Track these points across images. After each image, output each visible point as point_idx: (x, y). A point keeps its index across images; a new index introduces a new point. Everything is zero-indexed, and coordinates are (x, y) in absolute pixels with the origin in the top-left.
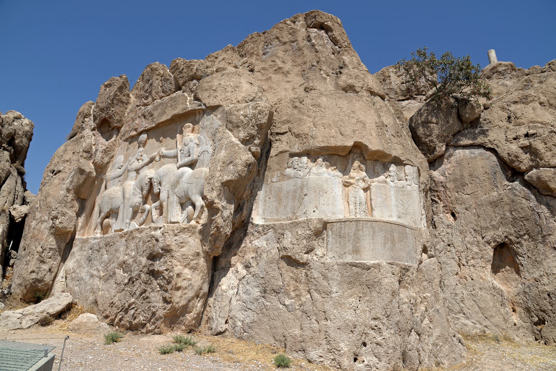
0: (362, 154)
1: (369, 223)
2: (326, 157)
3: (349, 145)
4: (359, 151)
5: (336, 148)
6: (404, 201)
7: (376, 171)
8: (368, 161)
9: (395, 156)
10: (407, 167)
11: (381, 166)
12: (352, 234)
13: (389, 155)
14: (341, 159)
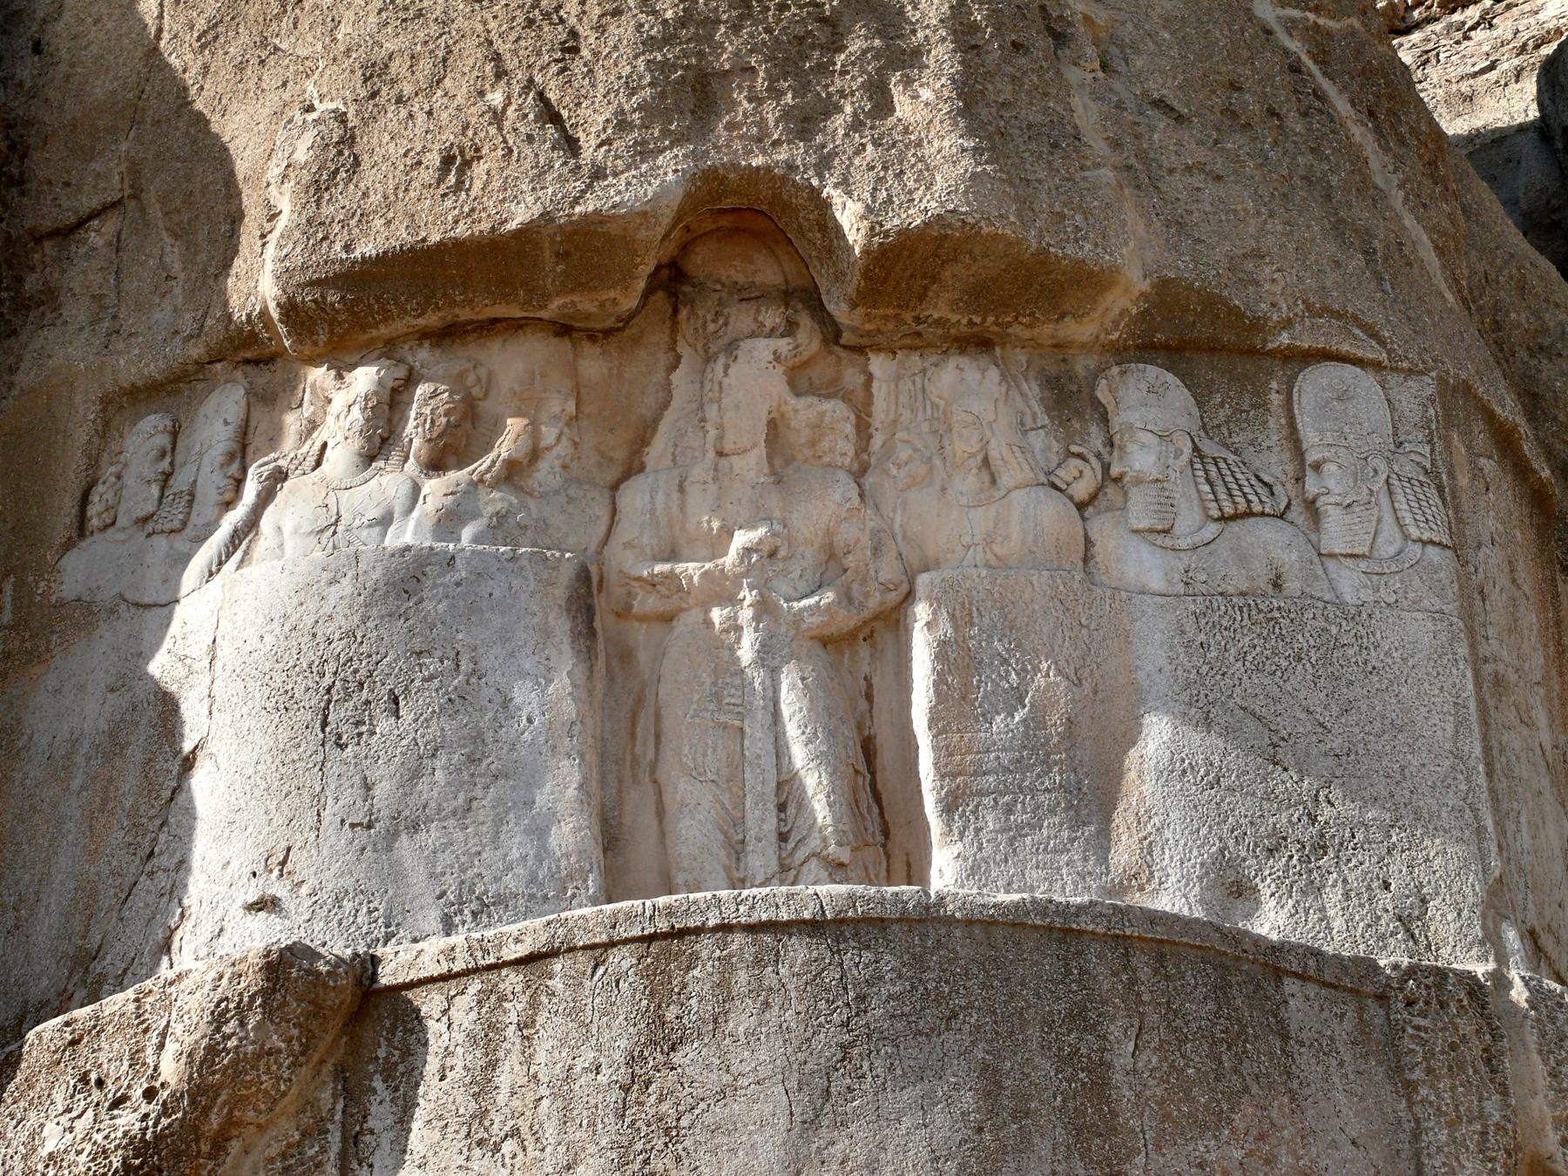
1: (799, 951)
8: (878, 364)
10: (1315, 384)
12: (597, 1090)
14: (593, 364)
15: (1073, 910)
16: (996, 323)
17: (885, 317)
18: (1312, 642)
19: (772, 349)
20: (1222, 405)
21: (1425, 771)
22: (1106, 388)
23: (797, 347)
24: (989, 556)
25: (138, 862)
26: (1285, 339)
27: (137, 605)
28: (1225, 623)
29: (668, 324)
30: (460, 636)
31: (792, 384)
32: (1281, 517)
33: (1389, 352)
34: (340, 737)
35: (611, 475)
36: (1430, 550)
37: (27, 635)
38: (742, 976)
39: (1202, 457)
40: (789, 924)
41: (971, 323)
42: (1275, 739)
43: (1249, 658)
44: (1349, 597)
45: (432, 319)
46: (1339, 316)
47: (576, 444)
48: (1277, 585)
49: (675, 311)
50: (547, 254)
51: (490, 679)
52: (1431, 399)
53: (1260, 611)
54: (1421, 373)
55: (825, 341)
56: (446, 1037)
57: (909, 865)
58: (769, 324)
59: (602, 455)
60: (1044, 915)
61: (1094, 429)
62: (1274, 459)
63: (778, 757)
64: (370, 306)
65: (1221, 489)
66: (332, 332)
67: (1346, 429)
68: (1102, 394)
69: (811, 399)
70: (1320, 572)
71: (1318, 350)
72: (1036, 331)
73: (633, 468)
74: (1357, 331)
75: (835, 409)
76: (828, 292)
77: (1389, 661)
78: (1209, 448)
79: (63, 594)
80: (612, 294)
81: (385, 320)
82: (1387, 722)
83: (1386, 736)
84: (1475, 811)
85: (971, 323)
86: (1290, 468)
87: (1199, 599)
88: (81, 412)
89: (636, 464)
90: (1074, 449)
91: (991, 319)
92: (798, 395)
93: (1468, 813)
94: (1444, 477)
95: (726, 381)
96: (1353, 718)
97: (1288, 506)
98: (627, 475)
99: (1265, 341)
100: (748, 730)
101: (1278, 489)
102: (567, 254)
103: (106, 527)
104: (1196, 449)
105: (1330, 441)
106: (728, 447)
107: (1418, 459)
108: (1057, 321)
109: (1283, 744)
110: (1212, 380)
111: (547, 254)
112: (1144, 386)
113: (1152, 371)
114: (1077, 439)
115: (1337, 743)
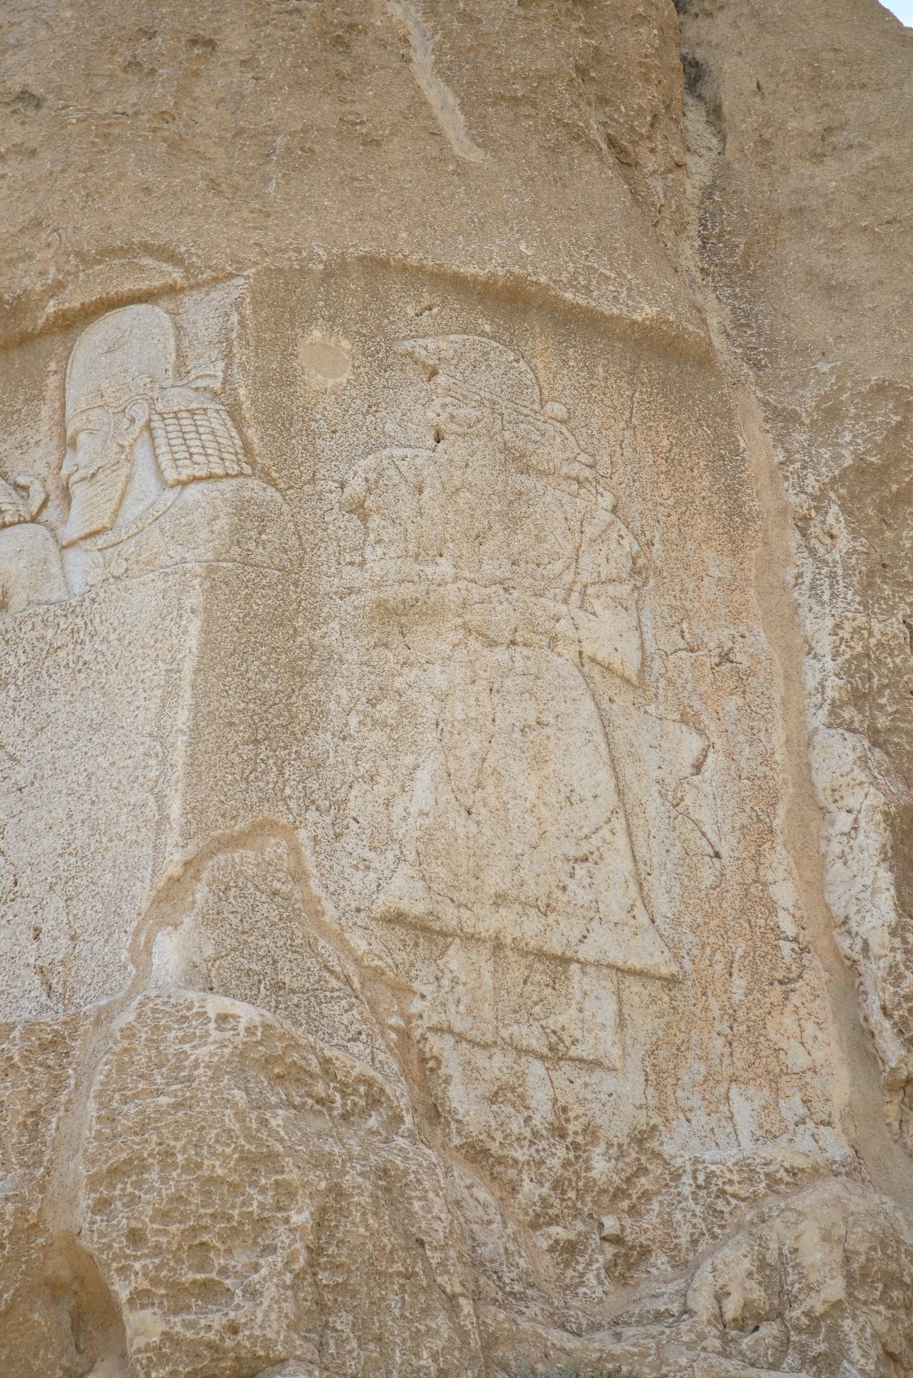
18: (23, 659)
21: (113, 770)
26: (51, 307)
32: (34, 520)
33: (187, 270)
36: (193, 492)
44: (78, 582)
46: (112, 252)
52: (237, 305)
54: (231, 276)
62: (40, 452)
67: (105, 385)
70: (55, 569)
71: (95, 303)
74: (147, 261)
77: (104, 647)
82: (85, 726)
83: (80, 744)
84: (160, 798)
94: (242, 391)
96: (43, 738)
97: (44, 505)
105: (84, 407)
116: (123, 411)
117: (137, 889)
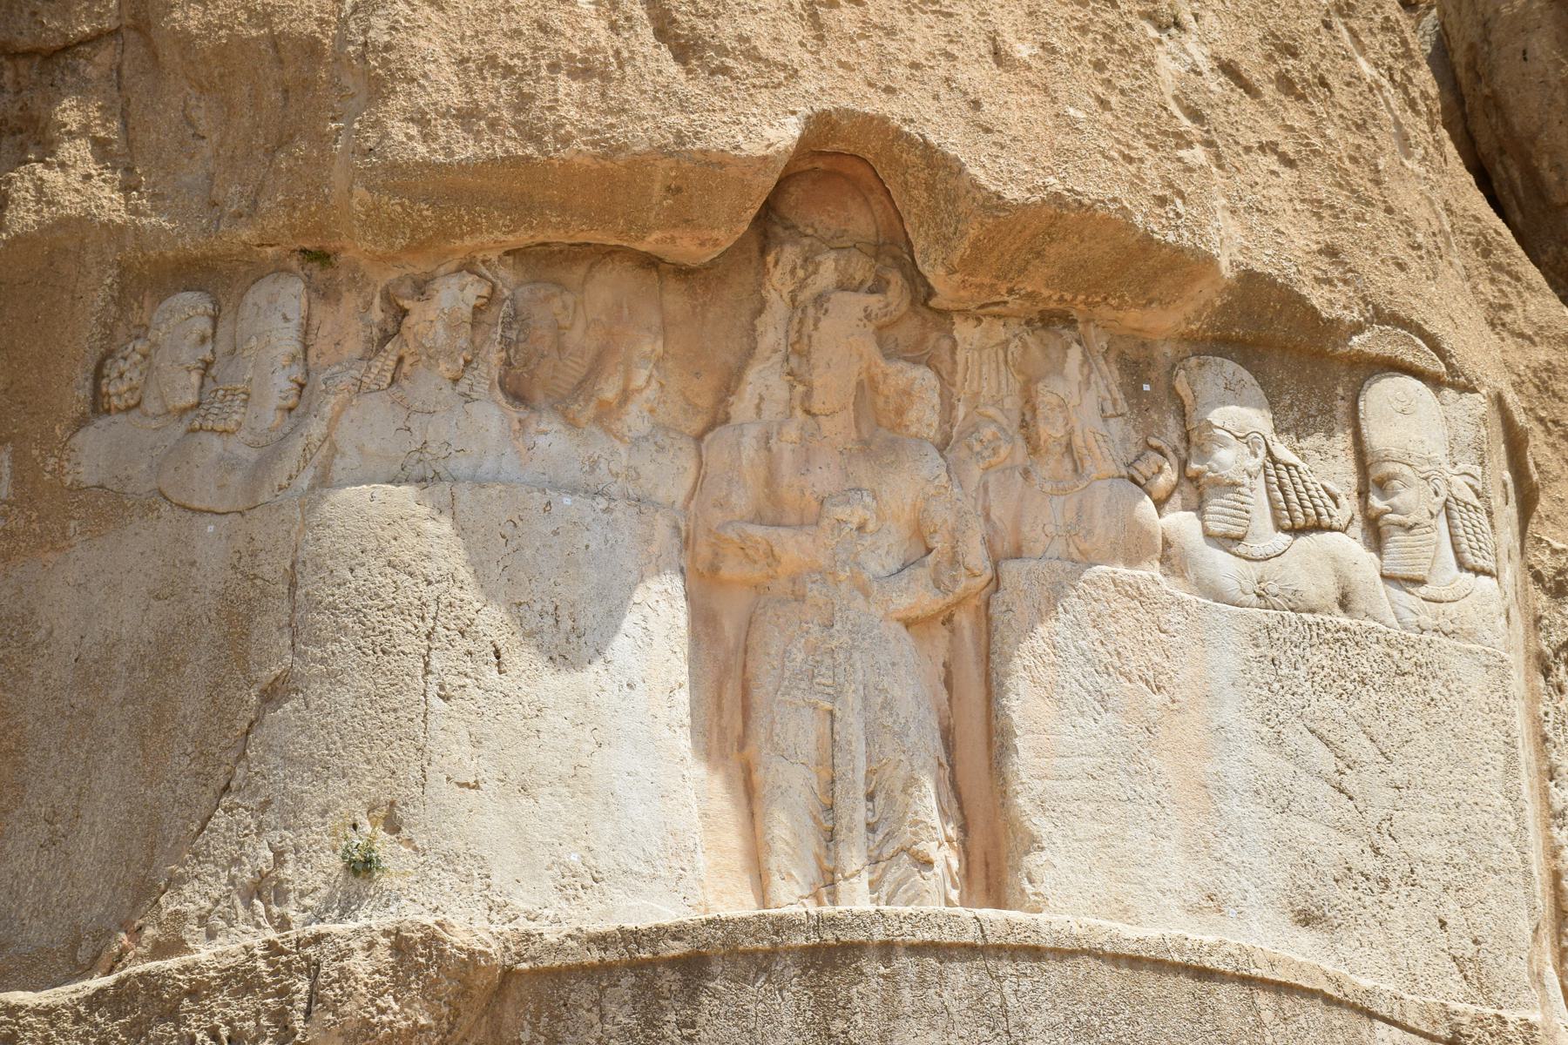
0: (893, 253)
1: (959, 973)
2: (507, 277)
3: (754, 148)
4: (862, 222)
5: (616, 180)
6: (1358, 746)
7: (1050, 430)
8: (964, 331)
9: (1249, 278)
11: (1109, 378)
13: (1187, 265)
14: (676, 300)
15: (1206, 949)
16: (1085, 302)
17: (981, 286)
19: (863, 305)
20: (1291, 406)
22: (1184, 380)
23: (887, 306)
24: (1072, 549)
25: (210, 794)
27: (185, 508)
28: (1294, 638)
29: (754, 264)
30: (558, 589)
31: (881, 344)
32: (1344, 531)
34: (442, 687)
35: (697, 424)
37: (34, 515)
38: (907, 994)
39: (1275, 462)
40: (950, 946)
41: (1061, 299)
42: (1341, 765)
43: (1317, 679)
45: (522, 238)
47: (662, 386)
48: (1344, 603)
49: (763, 251)
50: (657, 186)
51: (589, 638)
53: (1328, 630)
54: (1474, 391)
55: (912, 303)
56: (598, 1027)
57: (987, 865)
58: (859, 276)
59: (686, 399)
60: (1181, 953)
61: (1171, 421)
63: (867, 744)
64: (460, 217)
65: (1293, 497)
66: (412, 238)
68: (1181, 385)
69: (901, 365)
71: (1384, 359)
72: (1121, 314)
73: (719, 419)
74: (1419, 341)
75: (922, 377)
76: (924, 252)
78: (1283, 452)
79: (82, 478)
80: (715, 234)
81: (472, 233)
85: (1061, 299)
86: (1354, 480)
87: (1271, 612)
88: (94, 272)
89: (721, 416)
90: (1154, 442)
91: (1081, 297)
92: (887, 357)
93: (1517, 858)
95: (816, 335)
98: (711, 426)
99: (1336, 345)
100: (838, 714)
101: (1342, 500)
102: (679, 190)
103: (128, 409)
104: (1269, 453)
106: (816, 407)
107: (1471, 481)
108: (1145, 306)
109: (1348, 771)
110: (1282, 380)
111: (657, 186)
112: (1221, 382)
113: (1230, 366)
114: (1155, 431)
115: (1398, 775)
116: (1426, 479)
117: (1520, 923)
